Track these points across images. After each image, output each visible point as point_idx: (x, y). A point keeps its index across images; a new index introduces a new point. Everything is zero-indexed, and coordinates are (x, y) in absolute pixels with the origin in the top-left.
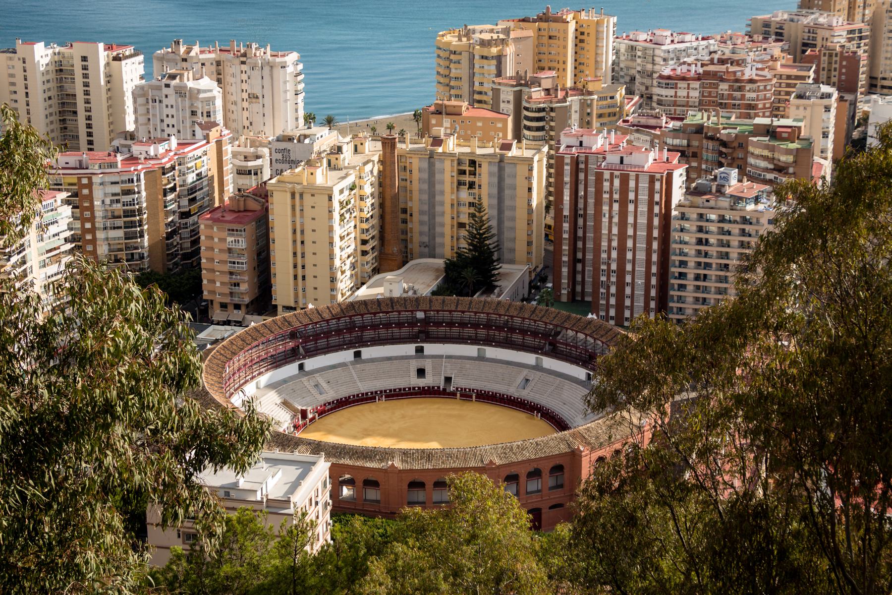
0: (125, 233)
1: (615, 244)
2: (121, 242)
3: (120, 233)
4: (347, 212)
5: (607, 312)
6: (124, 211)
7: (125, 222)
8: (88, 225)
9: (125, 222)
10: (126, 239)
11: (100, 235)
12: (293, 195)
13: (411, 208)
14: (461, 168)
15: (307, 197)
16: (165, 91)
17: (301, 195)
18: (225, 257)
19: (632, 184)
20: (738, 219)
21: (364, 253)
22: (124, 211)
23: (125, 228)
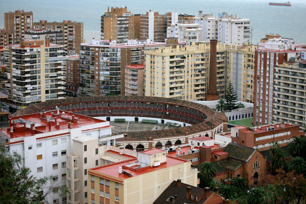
0: (110, 73)
1: (262, 86)
2: (108, 76)
3: (108, 73)
4: (177, 67)
5: (259, 120)
6: (110, 64)
7: (110, 68)
8: (97, 68)
9: (110, 68)
10: (110, 75)
11: (101, 73)
12: (151, 56)
13: (230, 76)
14: (249, 58)
15: (156, 57)
16: (176, 27)
17: (154, 56)
18: (132, 82)
19: (268, 57)
20: (299, 74)
21: (196, 91)
22: (111, 64)
23: (110, 70)
